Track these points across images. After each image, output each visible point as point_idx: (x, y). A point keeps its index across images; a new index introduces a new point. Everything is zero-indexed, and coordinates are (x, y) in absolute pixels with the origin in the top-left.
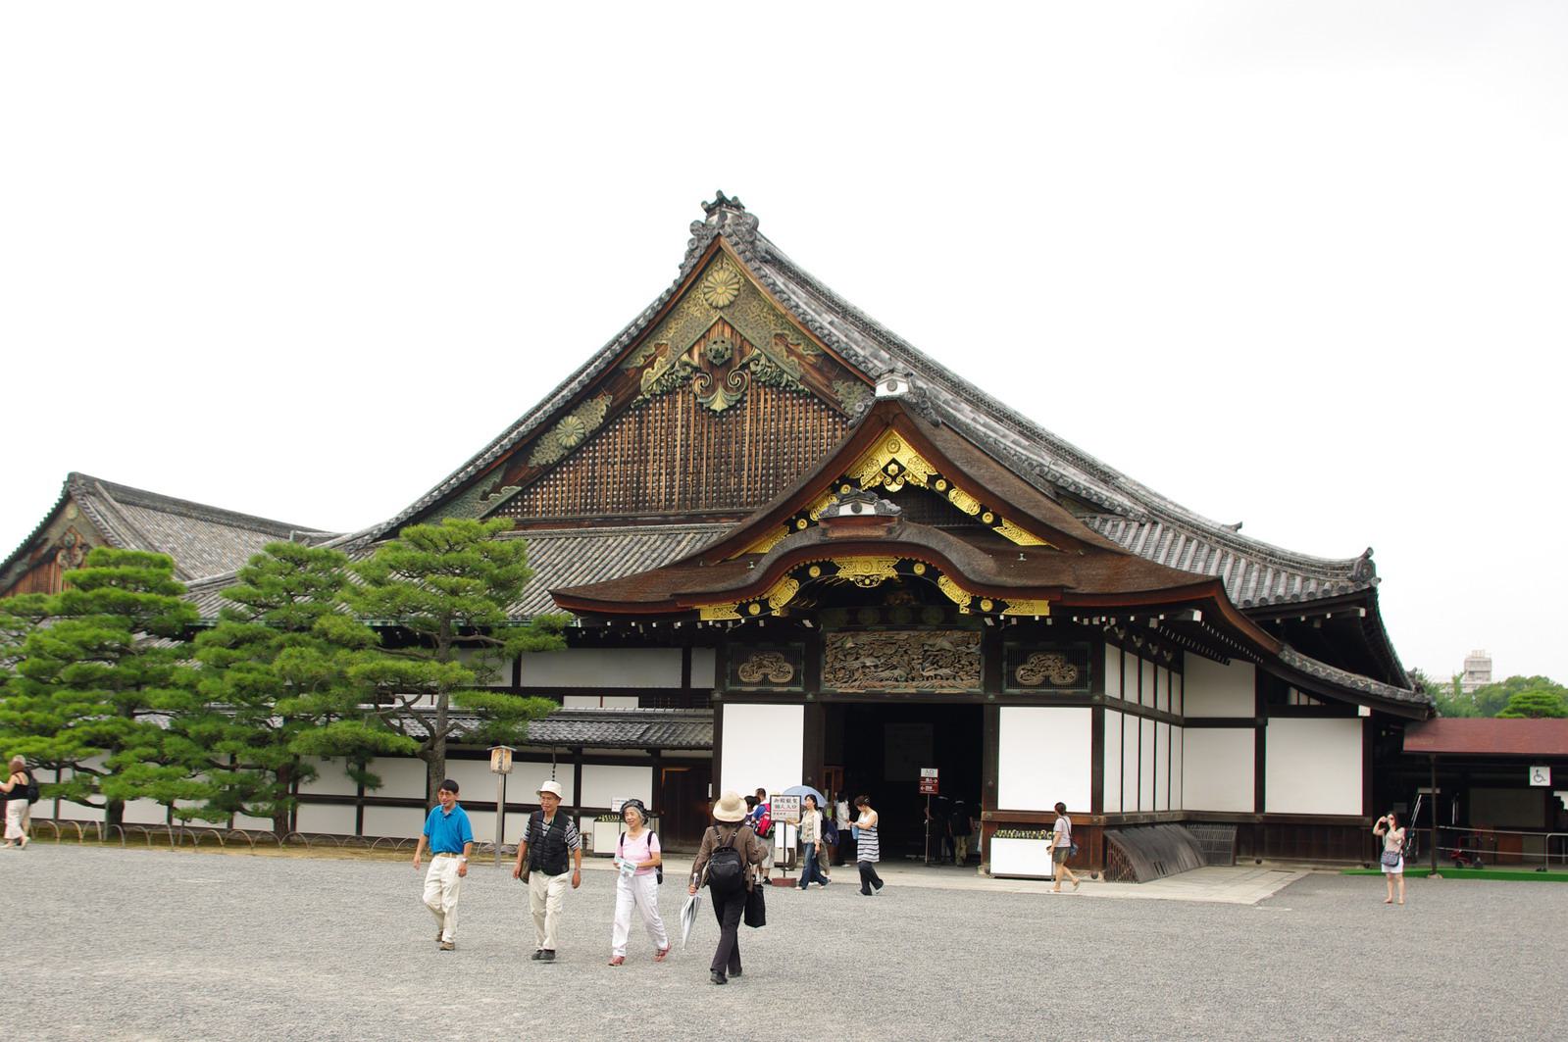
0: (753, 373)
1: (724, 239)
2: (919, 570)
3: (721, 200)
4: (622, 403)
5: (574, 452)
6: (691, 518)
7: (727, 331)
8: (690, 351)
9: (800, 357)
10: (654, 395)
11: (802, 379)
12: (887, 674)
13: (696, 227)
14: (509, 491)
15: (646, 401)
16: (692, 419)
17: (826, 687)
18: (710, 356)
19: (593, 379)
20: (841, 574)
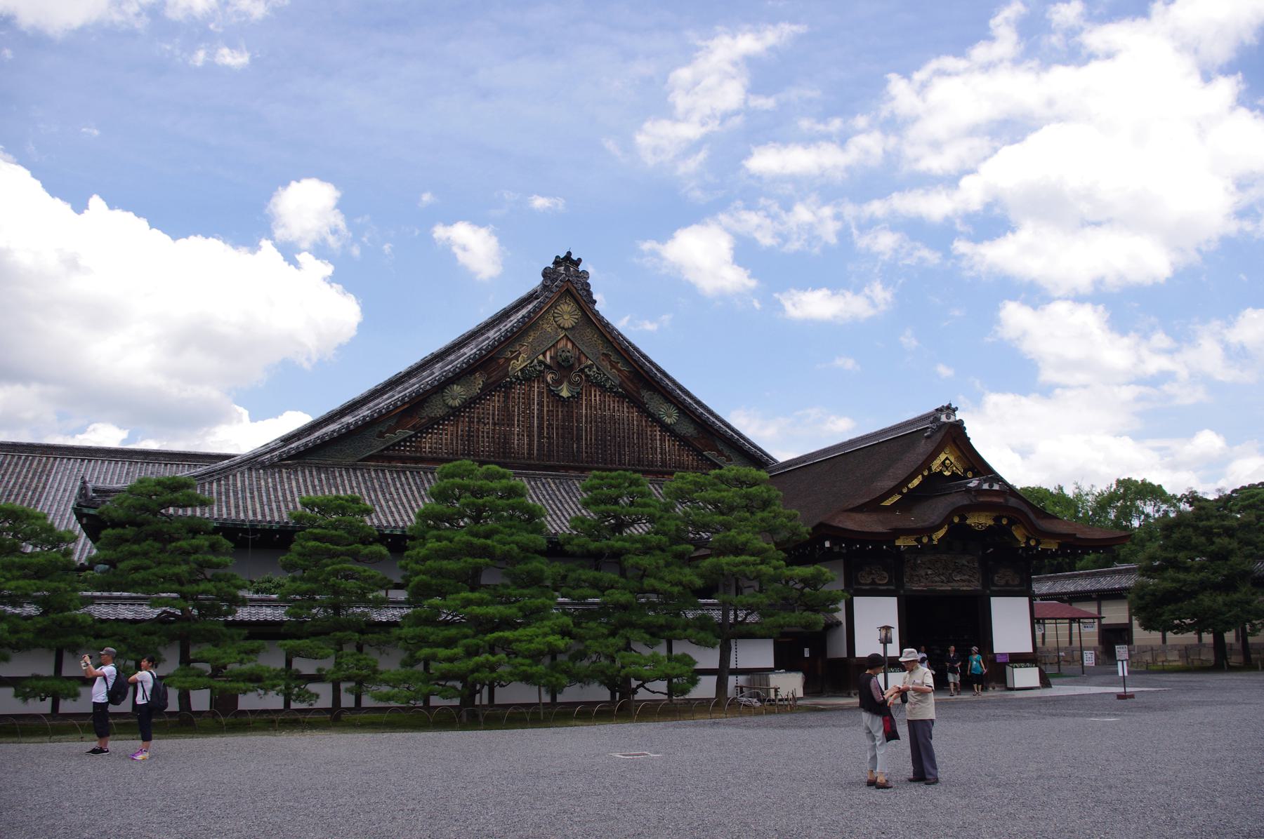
0: (587, 376)
1: (565, 281)
2: (1004, 522)
3: (568, 256)
4: (493, 383)
5: (455, 413)
6: (546, 468)
7: (570, 346)
8: (544, 354)
9: (619, 370)
10: (518, 378)
11: (620, 385)
12: (937, 579)
13: (546, 273)
14: (401, 433)
15: (511, 382)
16: (545, 400)
17: (908, 586)
18: (559, 359)
19: (477, 361)
20: (968, 522)
